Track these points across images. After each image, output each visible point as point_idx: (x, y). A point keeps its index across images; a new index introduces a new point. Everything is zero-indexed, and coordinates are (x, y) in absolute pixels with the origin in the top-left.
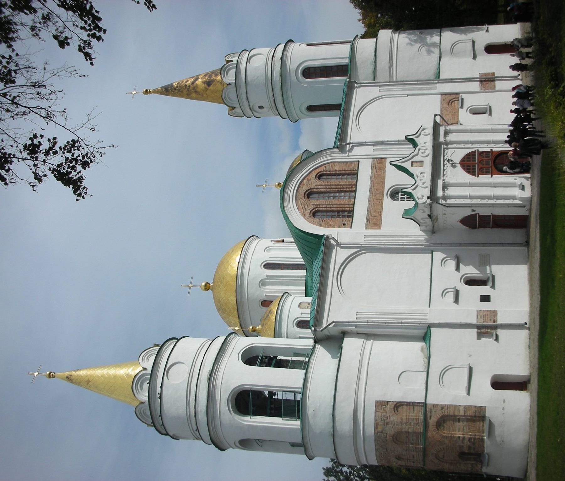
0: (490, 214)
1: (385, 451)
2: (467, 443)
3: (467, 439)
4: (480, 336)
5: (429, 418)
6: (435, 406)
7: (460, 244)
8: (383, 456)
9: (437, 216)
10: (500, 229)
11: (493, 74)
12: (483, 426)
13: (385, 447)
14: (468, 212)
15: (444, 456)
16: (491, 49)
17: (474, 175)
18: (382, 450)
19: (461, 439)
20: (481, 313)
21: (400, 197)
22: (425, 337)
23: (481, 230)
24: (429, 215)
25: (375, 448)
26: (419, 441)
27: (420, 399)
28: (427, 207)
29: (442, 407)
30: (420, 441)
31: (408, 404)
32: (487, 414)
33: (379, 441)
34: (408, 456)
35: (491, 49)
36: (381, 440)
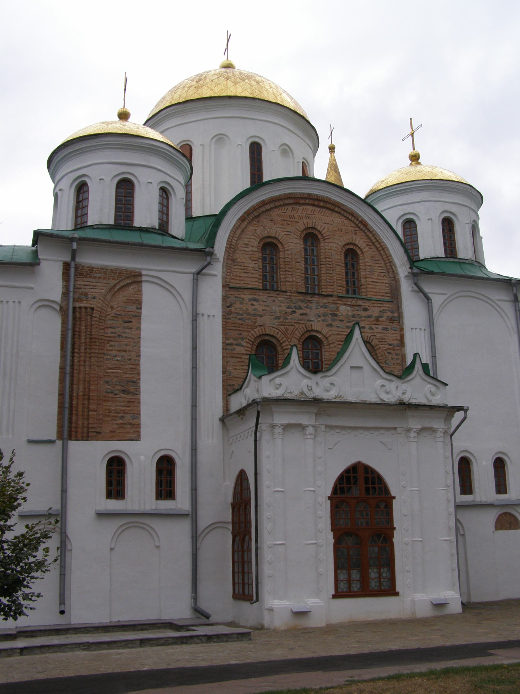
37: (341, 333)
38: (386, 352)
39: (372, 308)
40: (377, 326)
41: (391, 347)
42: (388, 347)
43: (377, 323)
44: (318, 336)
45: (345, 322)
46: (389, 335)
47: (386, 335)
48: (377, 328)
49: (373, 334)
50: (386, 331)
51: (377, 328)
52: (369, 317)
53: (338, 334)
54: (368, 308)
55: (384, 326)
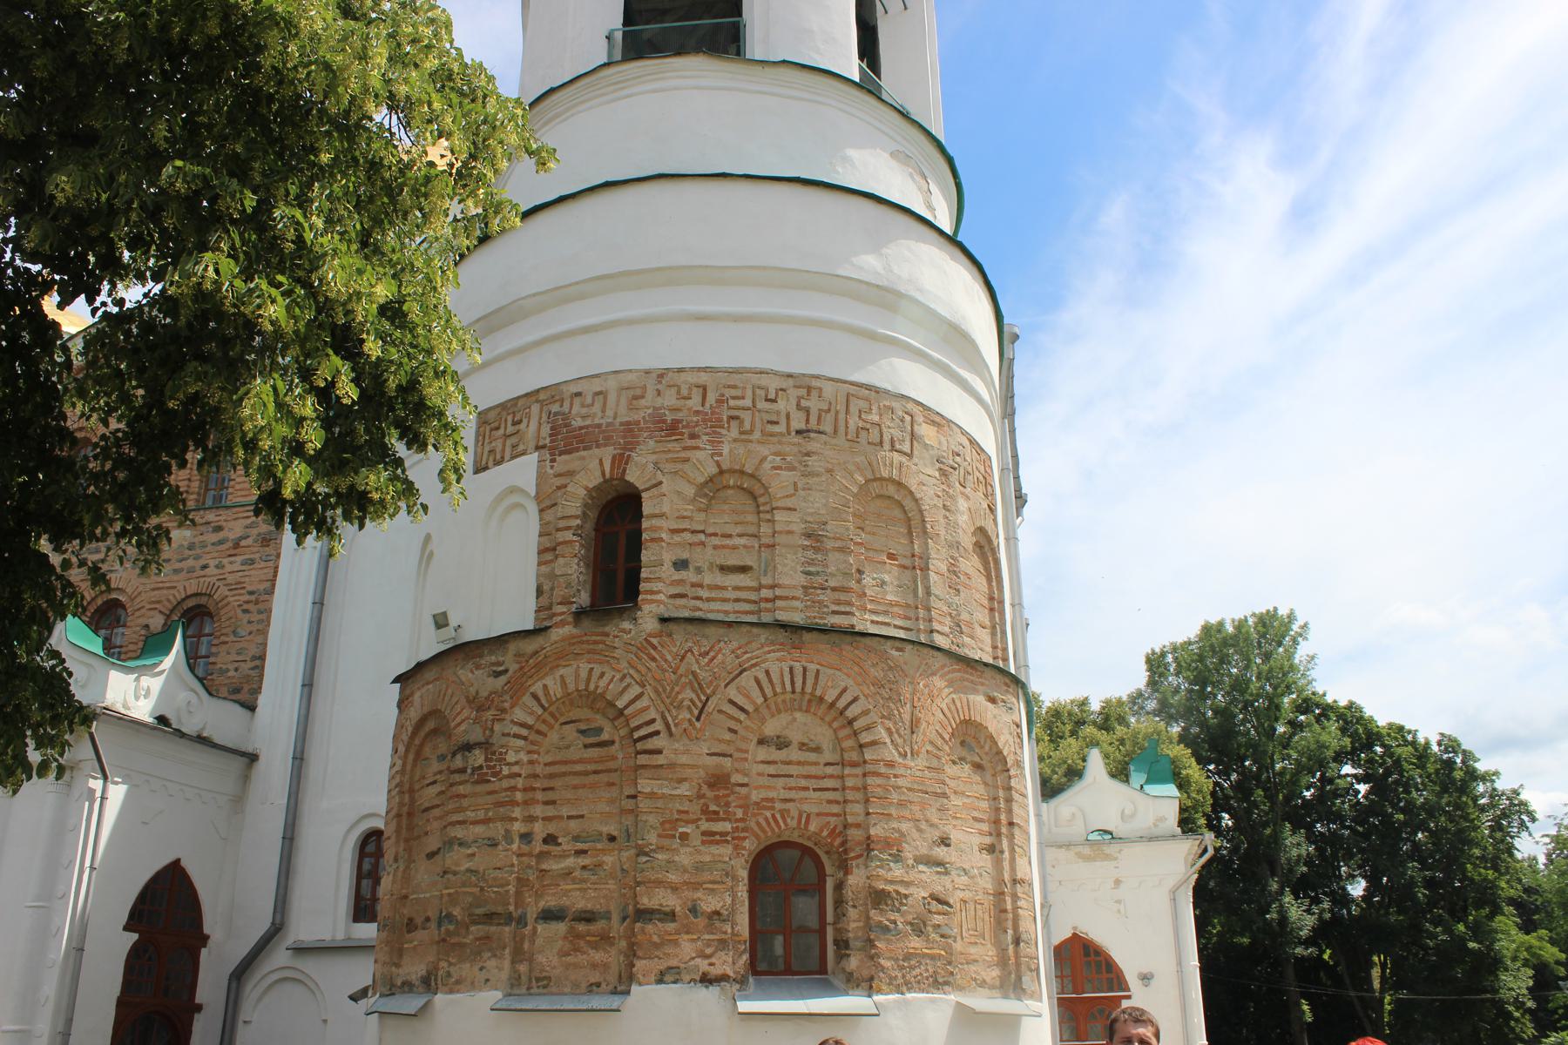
1: (798, 422)
2: (922, 884)
3: (938, 889)
8: (748, 402)
9: (1116, 859)
12: (983, 984)
13: (827, 427)
15: (782, 743)
18: (807, 411)
19: (941, 852)
25: (817, 377)
26: (875, 618)
28: (1155, 825)
30: (872, 622)
33: (863, 404)
34: (743, 541)
36: (876, 418)
37: (161, 585)
38: (239, 611)
39: (231, 524)
40: (232, 559)
41: (253, 598)
42: (247, 597)
43: (232, 552)
44: (121, 598)
45: (173, 561)
46: (252, 572)
47: (246, 573)
48: (231, 563)
49: (221, 577)
50: (251, 564)
51: (231, 563)
52: (221, 542)
53: (154, 589)
54: (224, 524)
55: (247, 557)
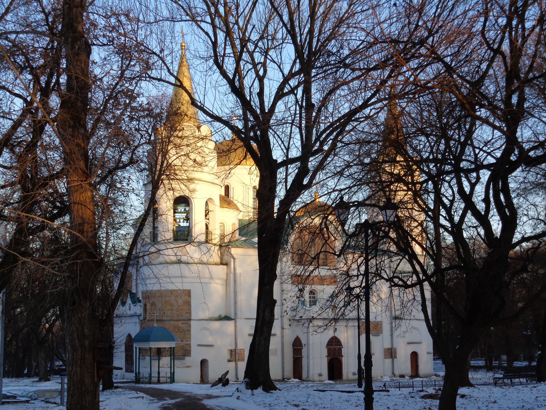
0: (303, 355)
4: (231, 351)
5: (182, 322)
6: (190, 326)
7: (282, 337)
10: (292, 362)
11: (396, 357)
14: (304, 341)
16: (414, 356)
17: (328, 345)
20: (242, 352)
21: (312, 296)
22: (227, 318)
23: (292, 350)
24: (301, 317)
27: (193, 317)
29: (189, 331)
31: (190, 309)
32: (187, 358)
35: (414, 356)
